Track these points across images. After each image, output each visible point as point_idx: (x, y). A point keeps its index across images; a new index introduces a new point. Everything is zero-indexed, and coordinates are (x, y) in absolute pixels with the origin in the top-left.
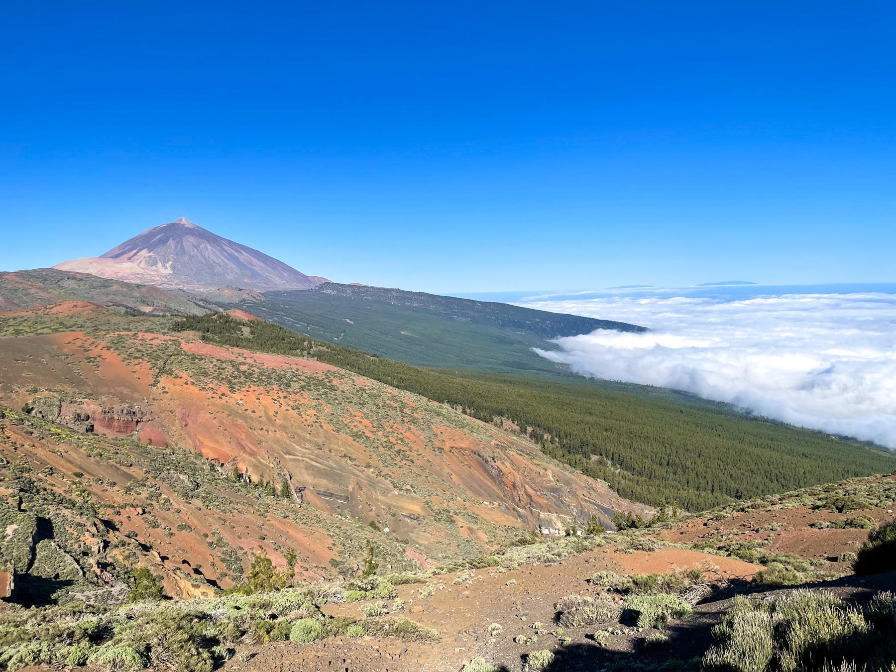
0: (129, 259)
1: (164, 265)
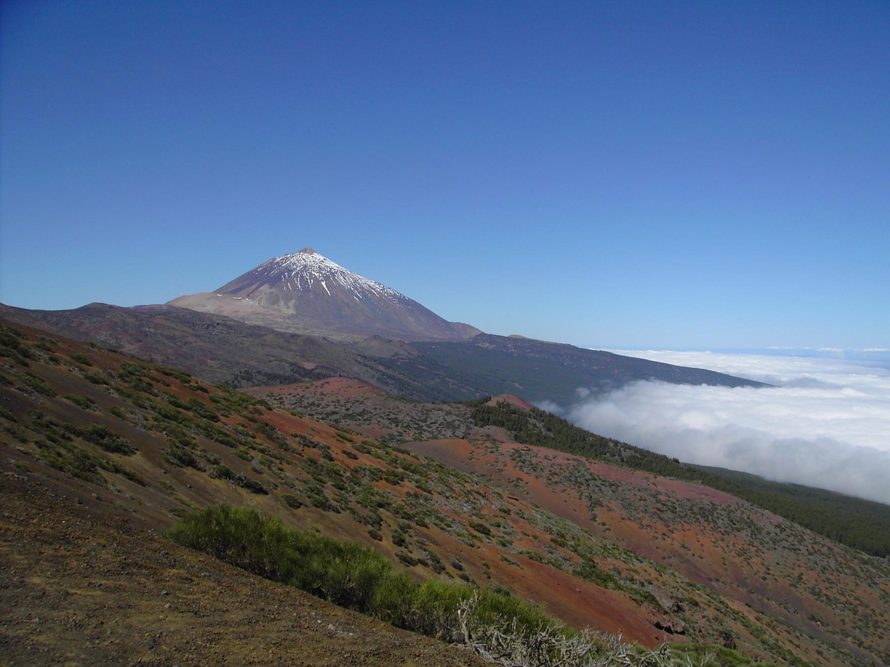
1: (286, 304)
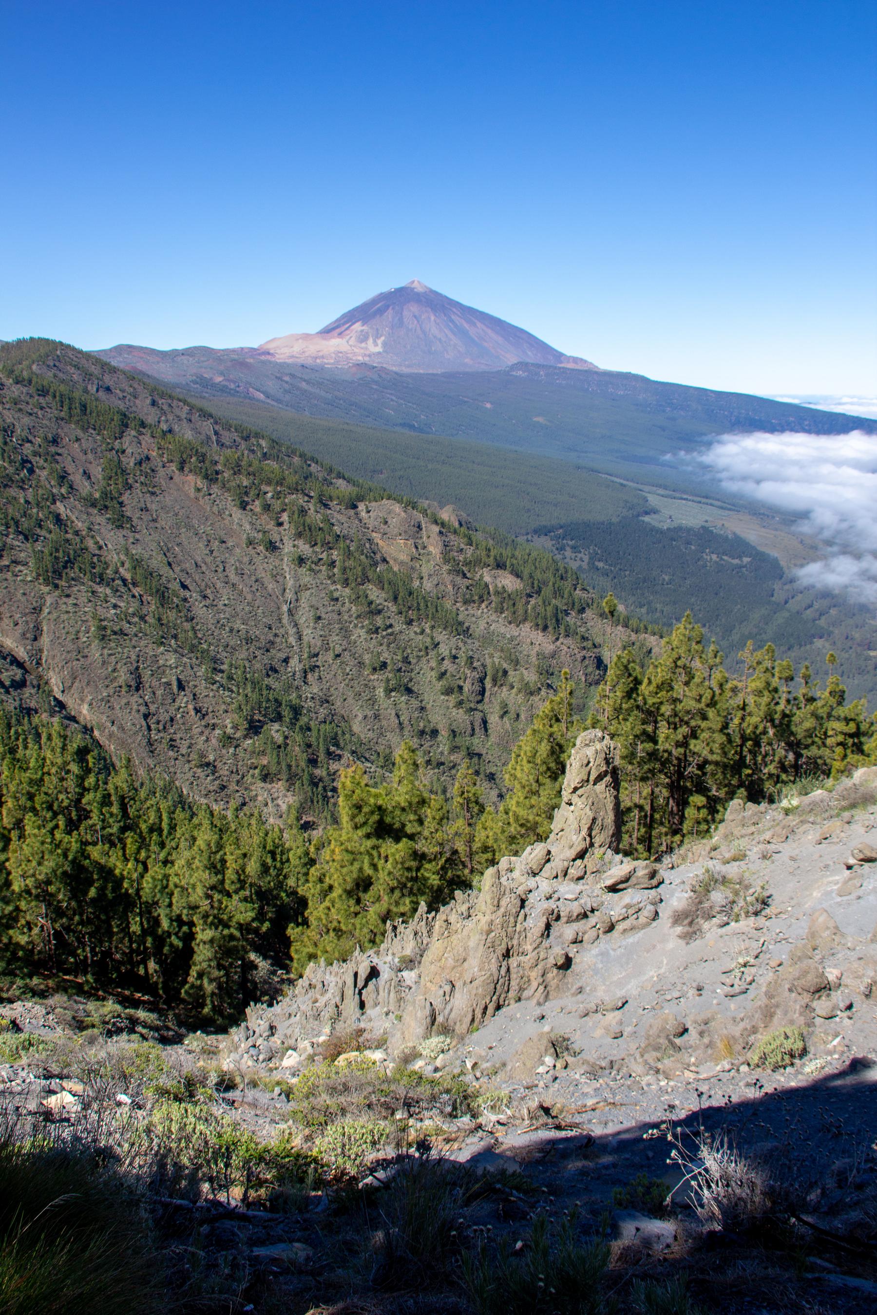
0: (340, 334)
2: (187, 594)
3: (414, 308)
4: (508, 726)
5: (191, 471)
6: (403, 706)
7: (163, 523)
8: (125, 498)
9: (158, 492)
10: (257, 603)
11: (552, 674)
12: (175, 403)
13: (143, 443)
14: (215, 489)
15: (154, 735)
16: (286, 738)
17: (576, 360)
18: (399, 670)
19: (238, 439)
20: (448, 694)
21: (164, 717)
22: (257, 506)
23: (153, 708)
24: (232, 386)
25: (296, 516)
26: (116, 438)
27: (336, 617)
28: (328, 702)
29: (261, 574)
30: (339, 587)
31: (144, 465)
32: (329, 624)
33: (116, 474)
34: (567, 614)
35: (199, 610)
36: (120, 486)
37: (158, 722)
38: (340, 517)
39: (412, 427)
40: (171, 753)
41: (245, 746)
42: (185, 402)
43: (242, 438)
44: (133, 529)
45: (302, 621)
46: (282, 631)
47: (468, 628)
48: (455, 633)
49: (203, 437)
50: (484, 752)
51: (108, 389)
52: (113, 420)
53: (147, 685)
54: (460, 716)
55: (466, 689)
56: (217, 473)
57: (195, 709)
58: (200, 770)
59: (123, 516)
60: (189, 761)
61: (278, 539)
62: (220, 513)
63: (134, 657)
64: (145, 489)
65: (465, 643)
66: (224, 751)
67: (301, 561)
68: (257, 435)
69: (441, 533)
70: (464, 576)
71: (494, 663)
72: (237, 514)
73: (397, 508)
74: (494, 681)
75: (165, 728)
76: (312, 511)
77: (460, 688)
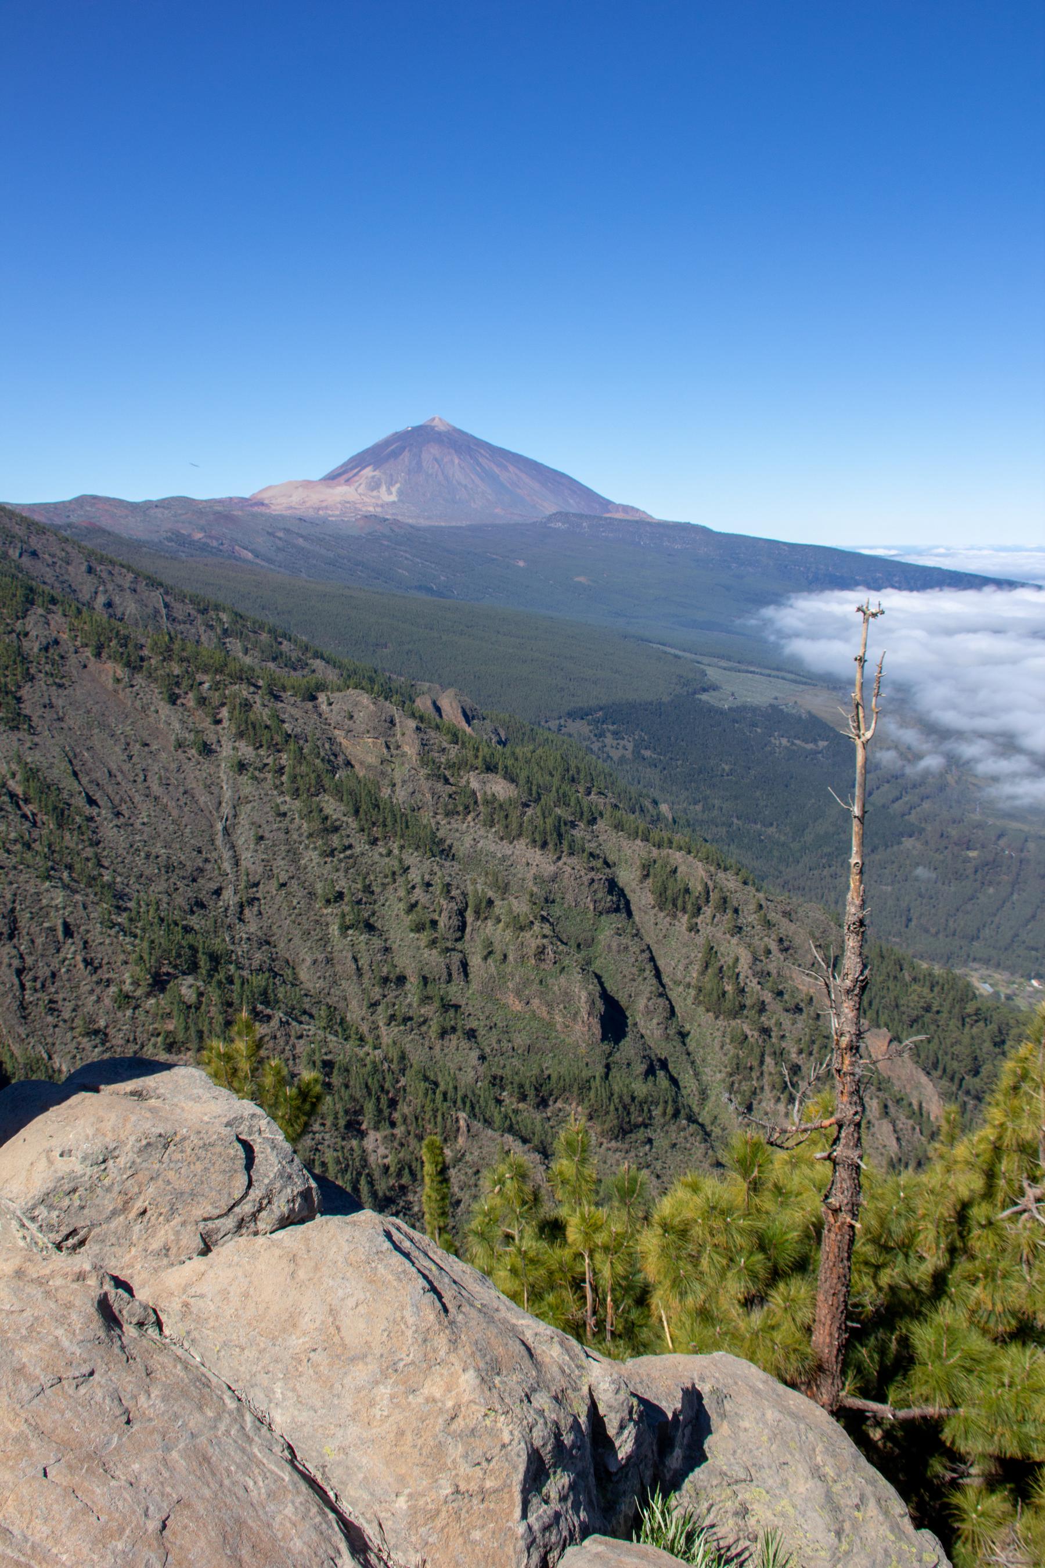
0: (347, 481)
2: (94, 811)
3: (434, 450)
4: (493, 970)
5: (110, 657)
6: (363, 947)
7: (72, 722)
8: (24, 692)
9: (67, 684)
10: (184, 821)
11: (553, 902)
12: (116, 570)
13: (52, 623)
14: (139, 679)
15: (29, 996)
16: (201, 994)
17: (626, 509)
18: (359, 902)
19: (193, 613)
20: (418, 931)
21: (43, 972)
22: (190, 700)
23: (29, 961)
24: (215, 544)
25: (237, 712)
26: (18, 618)
27: (282, 836)
28: (268, 943)
29: (191, 784)
30: (287, 798)
31: (51, 651)
32: (274, 845)
33: (15, 663)
34: (573, 825)
35: (109, 831)
36: (19, 678)
37: (35, 979)
38: (294, 713)
39: (429, 590)
40: (50, 1019)
41: (147, 1007)
42: (129, 568)
43: (199, 611)
44: (32, 730)
45: (240, 842)
46: (215, 855)
47: (450, 847)
48: (429, 854)
49: (150, 611)
50: (463, 1003)
51: (34, 554)
52: (14, 595)
53: (24, 932)
54: (433, 958)
55: (441, 924)
56: (142, 659)
57: (85, 960)
58: (86, 1040)
59: (19, 714)
60: (72, 1029)
61: (215, 741)
62: (144, 709)
63: (9, 896)
64: (50, 681)
65: (442, 866)
66: (120, 1014)
67: (241, 767)
68: (217, 608)
69: (418, 729)
70: (447, 781)
71: (476, 891)
72: (165, 709)
73: (365, 699)
74: (477, 912)
75: (43, 986)
76: (258, 705)
77: (434, 923)
